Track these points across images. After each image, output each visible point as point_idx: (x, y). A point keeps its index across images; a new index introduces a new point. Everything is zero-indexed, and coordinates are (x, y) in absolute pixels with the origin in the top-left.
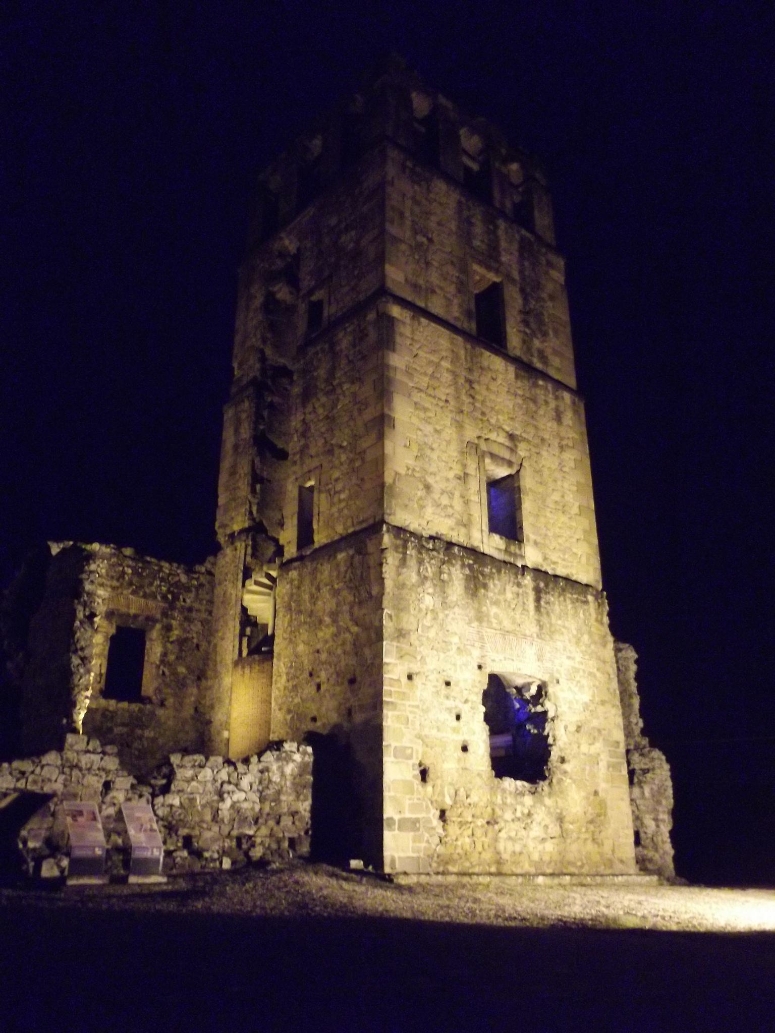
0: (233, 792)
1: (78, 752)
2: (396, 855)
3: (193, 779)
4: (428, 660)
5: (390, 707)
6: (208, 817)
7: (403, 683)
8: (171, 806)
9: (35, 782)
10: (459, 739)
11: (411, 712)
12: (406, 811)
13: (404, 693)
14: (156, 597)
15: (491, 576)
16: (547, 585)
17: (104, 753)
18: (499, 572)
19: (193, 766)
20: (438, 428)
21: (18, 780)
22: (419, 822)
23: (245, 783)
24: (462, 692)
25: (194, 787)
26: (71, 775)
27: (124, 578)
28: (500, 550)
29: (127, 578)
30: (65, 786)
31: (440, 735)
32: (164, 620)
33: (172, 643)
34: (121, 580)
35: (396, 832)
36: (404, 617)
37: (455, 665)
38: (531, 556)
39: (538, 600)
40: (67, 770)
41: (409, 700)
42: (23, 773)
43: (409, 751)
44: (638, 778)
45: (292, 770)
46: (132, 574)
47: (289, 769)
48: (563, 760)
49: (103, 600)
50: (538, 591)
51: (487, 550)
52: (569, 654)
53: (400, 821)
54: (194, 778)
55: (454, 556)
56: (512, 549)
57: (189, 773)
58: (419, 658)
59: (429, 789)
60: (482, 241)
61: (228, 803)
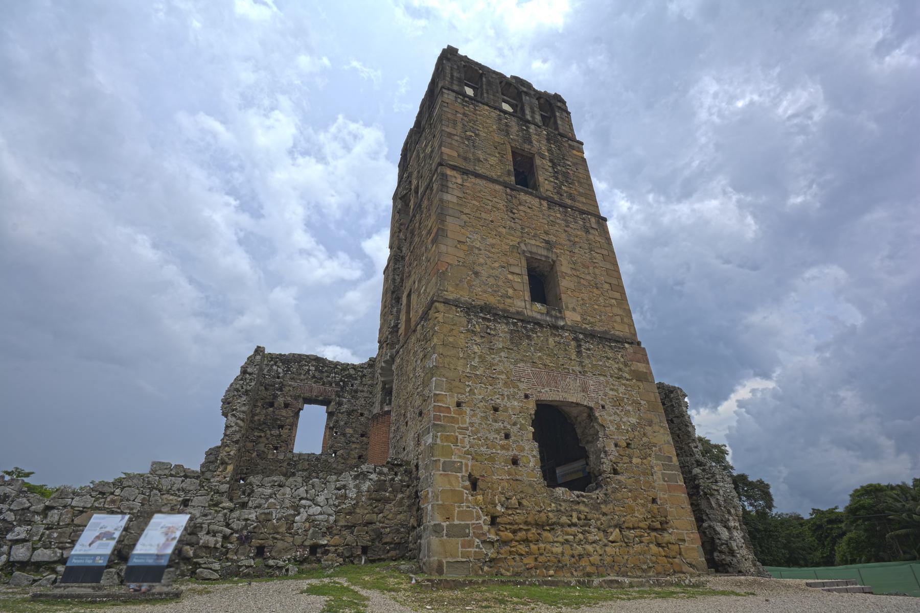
0: (309, 506)
1: (159, 476)
2: (444, 561)
3: (271, 497)
5: (440, 429)
6: (283, 530)
7: (452, 409)
8: (246, 520)
9: (113, 502)
10: (510, 453)
11: (460, 433)
12: (456, 520)
13: (453, 417)
14: (331, 385)
15: (532, 330)
16: (585, 335)
18: (541, 326)
21: (97, 499)
22: (469, 530)
23: (321, 499)
24: (510, 416)
25: (271, 503)
26: (149, 496)
27: (309, 373)
28: (542, 314)
30: (143, 504)
32: (337, 399)
33: (342, 413)
38: (572, 317)
40: (147, 492)
41: (458, 423)
42: (103, 494)
44: (703, 491)
45: (369, 487)
46: (315, 371)
48: (615, 472)
50: (576, 339)
51: (528, 312)
52: (612, 387)
53: (447, 526)
56: (553, 313)
57: (269, 491)
59: (480, 497)
60: (518, 136)
61: (304, 515)
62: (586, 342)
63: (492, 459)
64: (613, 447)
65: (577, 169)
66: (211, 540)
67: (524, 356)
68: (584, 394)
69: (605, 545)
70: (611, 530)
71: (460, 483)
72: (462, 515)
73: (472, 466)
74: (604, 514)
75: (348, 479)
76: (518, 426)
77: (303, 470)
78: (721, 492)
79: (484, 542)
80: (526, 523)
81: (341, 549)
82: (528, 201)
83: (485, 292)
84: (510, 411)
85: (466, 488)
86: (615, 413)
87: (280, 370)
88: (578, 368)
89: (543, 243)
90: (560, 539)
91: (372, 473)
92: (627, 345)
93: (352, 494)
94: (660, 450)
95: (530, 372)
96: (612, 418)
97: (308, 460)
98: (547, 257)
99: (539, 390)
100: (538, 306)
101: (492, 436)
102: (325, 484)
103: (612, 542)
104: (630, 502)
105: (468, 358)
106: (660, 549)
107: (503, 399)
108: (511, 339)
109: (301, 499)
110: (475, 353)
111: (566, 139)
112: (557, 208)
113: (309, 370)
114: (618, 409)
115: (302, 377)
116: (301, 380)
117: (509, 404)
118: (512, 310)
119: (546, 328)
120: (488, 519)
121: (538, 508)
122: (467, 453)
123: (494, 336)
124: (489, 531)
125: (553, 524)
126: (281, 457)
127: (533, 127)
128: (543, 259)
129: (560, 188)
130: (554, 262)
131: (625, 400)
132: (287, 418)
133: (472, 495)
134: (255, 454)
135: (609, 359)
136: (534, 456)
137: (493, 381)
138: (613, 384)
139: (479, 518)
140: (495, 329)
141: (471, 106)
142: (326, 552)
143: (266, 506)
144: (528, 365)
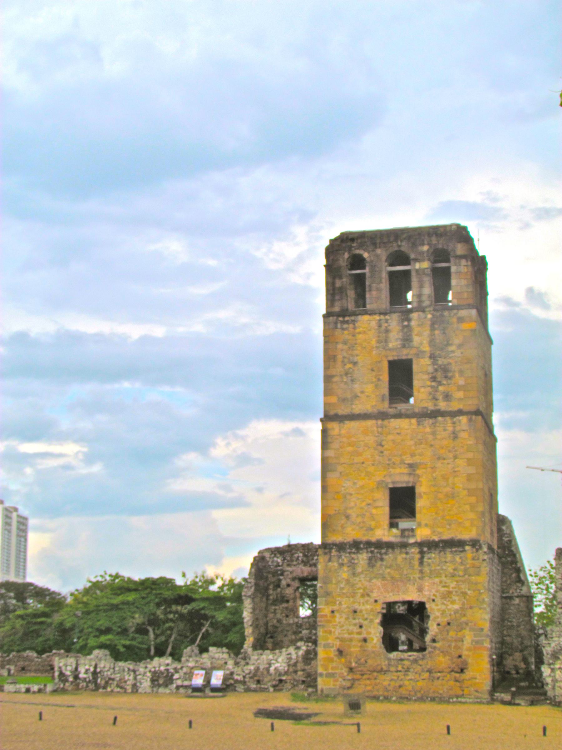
0: (275, 664)
2: (324, 687)
4: (343, 603)
6: (265, 673)
8: (250, 670)
9: (201, 664)
10: (361, 637)
11: (333, 628)
15: (386, 554)
16: (429, 548)
17: (223, 653)
19: (258, 655)
20: (355, 481)
23: (280, 660)
24: (363, 615)
28: (396, 536)
29: (300, 559)
31: (349, 636)
34: (298, 561)
35: (324, 678)
36: (329, 586)
37: (360, 603)
39: (422, 559)
43: (331, 645)
45: (302, 653)
46: (303, 556)
47: (301, 653)
48: (434, 641)
49: (291, 572)
50: (422, 553)
51: (386, 539)
52: (444, 584)
54: (258, 659)
55: (361, 549)
57: (256, 657)
58: (338, 602)
59: (343, 660)
62: (428, 553)
63: (351, 640)
64: (435, 626)
65: (462, 353)
66: (239, 678)
67: (378, 574)
68: (418, 593)
69: (418, 681)
70: (424, 673)
71: (332, 653)
72: (332, 668)
73: (339, 645)
74: (420, 665)
75: (292, 650)
76: (369, 620)
77: (307, 629)
78: (553, 645)
79: (344, 680)
80: (369, 671)
81: (292, 682)
82: (397, 427)
83: (353, 530)
84: (364, 612)
85: (335, 655)
86: (443, 603)
87: (279, 560)
88: (417, 575)
89: (407, 468)
90: (388, 678)
91: (303, 646)
92: (467, 548)
93: (294, 656)
94: (475, 624)
95: (380, 584)
96: (439, 607)
97: (308, 622)
98: (409, 482)
99: (385, 596)
100: (394, 530)
101: (351, 628)
102: (281, 652)
103: (423, 679)
104: (441, 658)
105: (339, 582)
106: (458, 684)
107: (360, 605)
108: (369, 564)
109: (271, 660)
110: (343, 579)
111: (455, 311)
112: (427, 422)
113: (298, 557)
114: (446, 600)
115: (295, 563)
116: (295, 565)
117: (363, 608)
118: (373, 539)
119: (397, 548)
120: (347, 670)
121: (376, 664)
122: (337, 638)
123: (357, 564)
124: (348, 675)
125: (386, 671)
126: (291, 621)
127: (414, 315)
128: (404, 485)
129: (437, 391)
130: (415, 484)
131: (454, 593)
132: (290, 594)
133: (339, 659)
134: (275, 621)
135: (446, 562)
136: (377, 637)
137: (354, 595)
138: (445, 583)
139: (342, 669)
140: (358, 559)
141: (351, 326)
142: (286, 682)
143: (257, 663)
144: (380, 580)
